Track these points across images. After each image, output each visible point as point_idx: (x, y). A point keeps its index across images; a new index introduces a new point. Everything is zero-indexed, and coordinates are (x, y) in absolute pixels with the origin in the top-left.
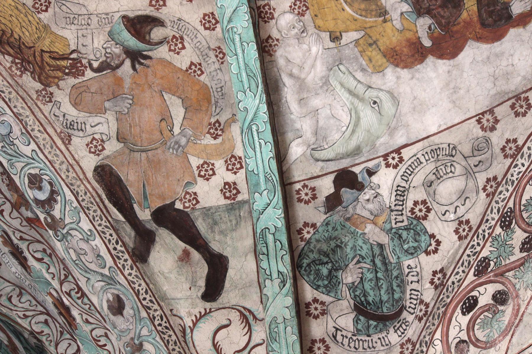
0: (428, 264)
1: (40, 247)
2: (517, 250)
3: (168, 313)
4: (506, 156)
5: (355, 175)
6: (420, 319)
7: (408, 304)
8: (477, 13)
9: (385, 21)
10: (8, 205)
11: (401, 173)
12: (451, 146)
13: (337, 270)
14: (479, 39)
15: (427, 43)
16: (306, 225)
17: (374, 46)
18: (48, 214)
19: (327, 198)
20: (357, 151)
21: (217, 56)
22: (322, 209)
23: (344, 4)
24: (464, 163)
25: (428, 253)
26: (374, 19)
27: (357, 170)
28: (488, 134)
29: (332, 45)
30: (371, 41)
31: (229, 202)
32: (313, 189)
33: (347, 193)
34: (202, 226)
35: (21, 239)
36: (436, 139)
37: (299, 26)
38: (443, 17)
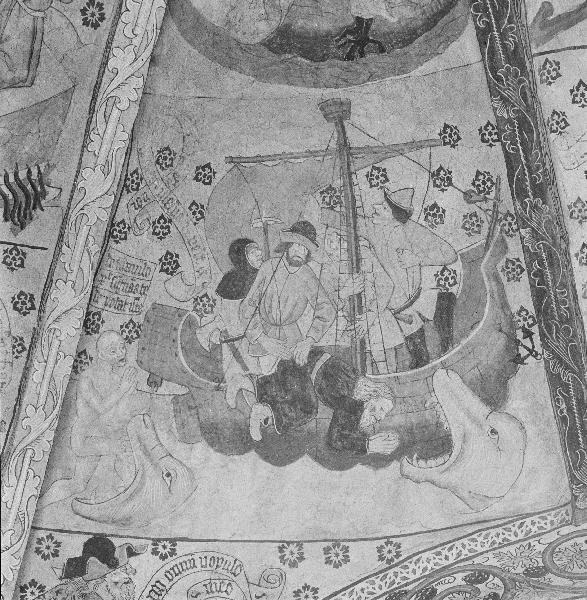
8: (327, 431)
9: (218, 389)
11: (167, 568)
12: (238, 563)
14: (318, 459)
15: (256, 436)
16: (33, 583)
17: (193, 411)
19: (70, 561)
20: (126, 521)
21: (14, 347)
22: (59, 572)
23: (179, 349)
24: (245, 588)
26: (206, 381)
28: (286, 568)
29: (146, 388)
30: (192, 404)
32: (58, 544)
33: (94, 565)
37: (120, 353)
38: (286, 415)
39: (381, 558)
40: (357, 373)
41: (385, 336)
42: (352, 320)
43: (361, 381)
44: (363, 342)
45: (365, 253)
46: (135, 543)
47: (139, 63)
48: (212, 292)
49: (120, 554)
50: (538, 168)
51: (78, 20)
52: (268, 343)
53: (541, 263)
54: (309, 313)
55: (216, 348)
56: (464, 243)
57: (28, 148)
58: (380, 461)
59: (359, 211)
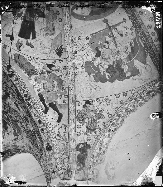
0: (101, 121)
1: (22, 105)
2: (120, 121)
3: (50, 124)
4: (120, 103)
5: (90, 102)
6: (99, 132)
7: (97, 128)
10: (16, 95)
13: (84, 119)
14: (118, 80)
15: (108, 78)
18: (28, 102)
20: (91, 97)
25: (102, 119)
27: (90, 101)
31: (64, 103)
33: (87, 105)
34: (58, 107)
35: (19, 103)
36: (107, 98)
39: (132, 93)
40: (121, 64)
41: (124, 56)
42: (118, 55)
43: (122, 65)
44: (121, 58)
45: (117, 43)
46: (93, 100)
47: (68, 26)
48: (95, 57)
49: (91, 103)
50: (138, 23)
51: (58, 21)
52: (106, 63)
53: (143, 38)
54: (111, 56)
55: (98, 66)
56: (133, 37)
57: (58, 44)
58: (128, 78)
59: (115, 37)
